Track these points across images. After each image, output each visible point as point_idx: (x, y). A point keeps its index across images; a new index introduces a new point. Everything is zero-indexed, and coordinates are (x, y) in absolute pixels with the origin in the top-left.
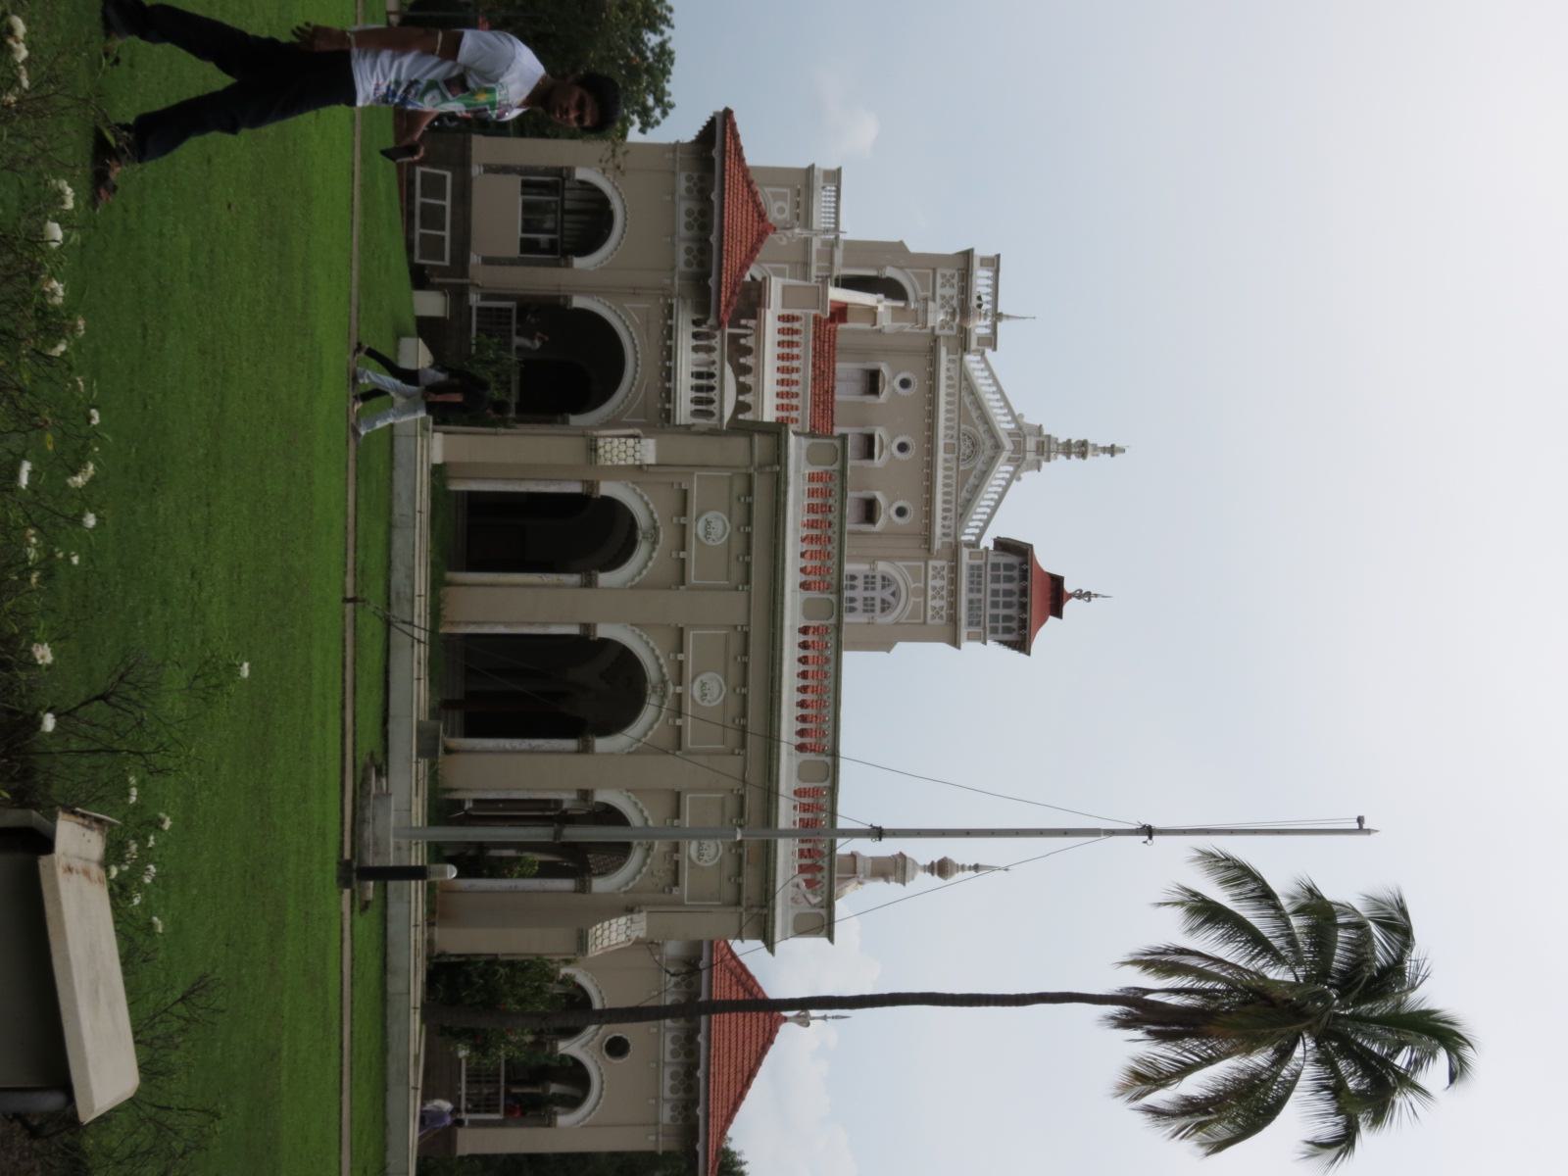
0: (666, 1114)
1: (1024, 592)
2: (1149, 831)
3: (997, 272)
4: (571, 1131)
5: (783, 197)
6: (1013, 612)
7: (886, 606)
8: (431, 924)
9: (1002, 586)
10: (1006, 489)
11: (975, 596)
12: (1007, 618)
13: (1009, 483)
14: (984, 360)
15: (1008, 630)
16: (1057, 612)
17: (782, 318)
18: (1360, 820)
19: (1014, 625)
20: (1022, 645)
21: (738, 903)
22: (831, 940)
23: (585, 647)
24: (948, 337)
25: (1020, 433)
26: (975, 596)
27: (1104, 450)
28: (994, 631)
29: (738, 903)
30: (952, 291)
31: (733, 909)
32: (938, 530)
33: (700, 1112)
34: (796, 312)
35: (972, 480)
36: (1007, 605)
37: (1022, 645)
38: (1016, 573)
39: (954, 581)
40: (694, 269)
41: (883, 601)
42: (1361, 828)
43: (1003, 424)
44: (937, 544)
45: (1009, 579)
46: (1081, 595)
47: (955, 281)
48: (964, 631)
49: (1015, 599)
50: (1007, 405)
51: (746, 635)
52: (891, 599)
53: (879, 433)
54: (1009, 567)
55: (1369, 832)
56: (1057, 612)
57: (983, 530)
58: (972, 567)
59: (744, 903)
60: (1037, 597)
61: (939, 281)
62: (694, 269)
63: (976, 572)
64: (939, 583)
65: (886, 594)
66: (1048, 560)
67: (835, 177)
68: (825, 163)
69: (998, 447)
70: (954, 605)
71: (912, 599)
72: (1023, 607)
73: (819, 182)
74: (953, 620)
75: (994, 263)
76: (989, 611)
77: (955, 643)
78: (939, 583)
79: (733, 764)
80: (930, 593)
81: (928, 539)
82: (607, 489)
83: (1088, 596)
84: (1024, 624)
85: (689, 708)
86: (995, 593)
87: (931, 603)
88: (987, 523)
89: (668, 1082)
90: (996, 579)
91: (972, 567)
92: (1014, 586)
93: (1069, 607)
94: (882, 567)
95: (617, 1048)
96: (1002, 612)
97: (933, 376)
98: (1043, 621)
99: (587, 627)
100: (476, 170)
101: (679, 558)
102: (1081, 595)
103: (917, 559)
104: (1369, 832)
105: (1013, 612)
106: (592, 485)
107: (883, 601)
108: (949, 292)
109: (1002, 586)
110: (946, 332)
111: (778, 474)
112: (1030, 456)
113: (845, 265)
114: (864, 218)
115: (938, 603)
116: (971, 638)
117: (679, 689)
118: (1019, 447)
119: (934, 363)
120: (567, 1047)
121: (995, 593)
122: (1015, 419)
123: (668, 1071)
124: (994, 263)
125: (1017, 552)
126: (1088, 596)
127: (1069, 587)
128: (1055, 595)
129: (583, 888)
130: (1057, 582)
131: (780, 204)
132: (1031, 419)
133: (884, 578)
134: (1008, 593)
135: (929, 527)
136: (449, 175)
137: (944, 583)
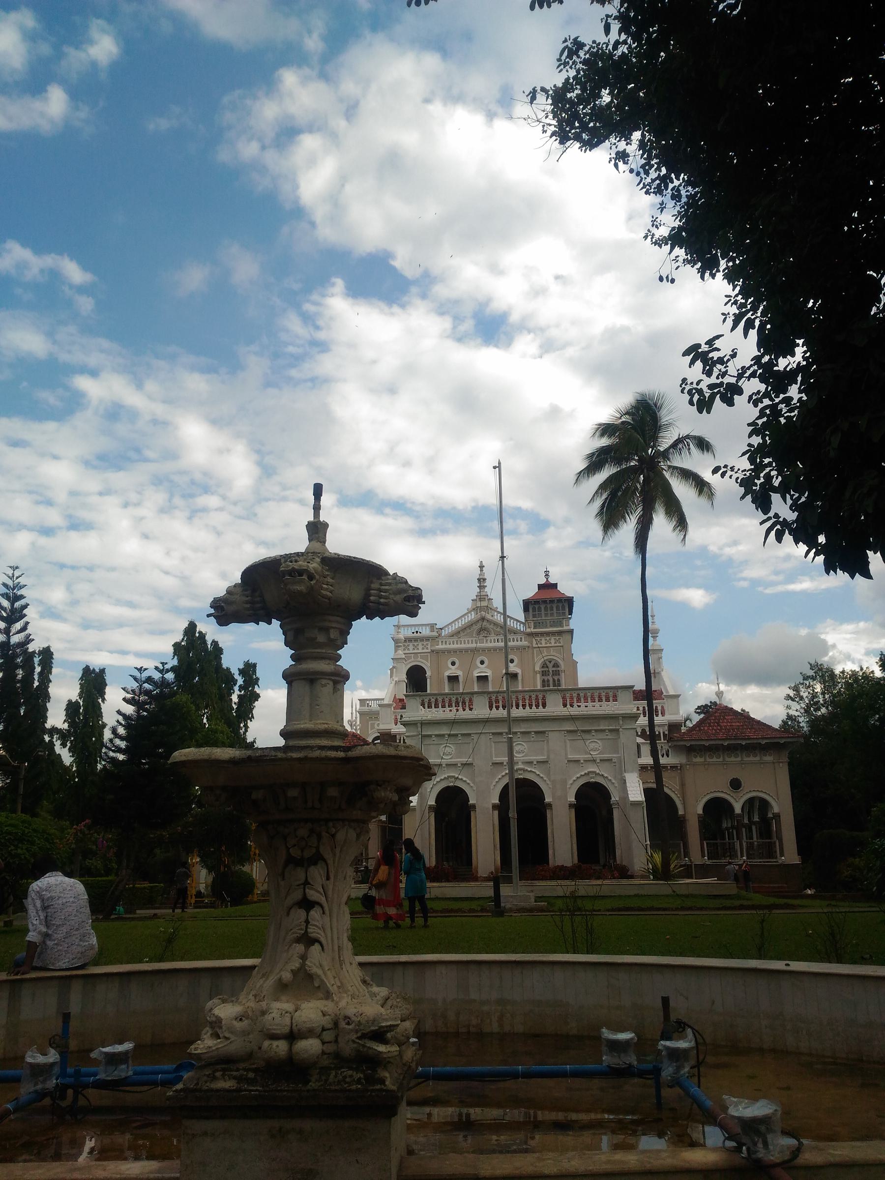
0: (768, 758)
1: (545, 602)
2: (502, 557)
4: (782, 804)
5: (372, 725)
7: (556, 665)
8: (632, 877)
9: (543, 612)
12: (558, 609)
15: (563, 609)
16: (555, 586)
18: (495, 468)
19: (560, 605)
20: (570, 601)
21: (618, 730)
23: (502, 807)
25: (475, 609)
27: (481, 570)
28: (564, 614)
29: (618, 730)
32: (519, 643)
33: (764, 742)
35: (498, 629)
36: (552, 609)
38: (537, 606)
39: (542, 634)
41: (553, 667)
42: (498, 467)
43: (473, 616)
44: (525, 643)
45: (540, 609)
46: (547, 575)
48: (565, 628)
49: (549, 606)
51: (493, 734)
52: (553, 663)
53: (476, 674)
55: (499, 463)
56: (555, 586)
58: (535, 627)
60: (548, 595)
64: (543, 642)
65: (550, 665)
66: (531, 592)
69: (483, 619)
70: (553, 634)
71: (552, 653)
72: (552, 601)
73: (366, 709)
74: (560, 633)
78: (543, 642)
79: (551, 735)
80: (548, 645)
81: (524, 648)
82: (432, 802)
85: (527, 758)
86: (546, 615)
89: (752, 758)
90: (540, 615)
91: (535, 627)
93: (552, 580)
94: (537, 668)
95: (736, 784)
97: (449, 651)
99: (495, 807)
102: (547, 575)
103: (533, 653)
104: (499, 463)
105: (554, 606)
106: (430, 807)
107: (553, 667)
109: (543, 612)
110: (429, 647)
111: (422, 724)
112: (484, 604)
115: (553, 641)
118: (481, 608)
119: (443, 651)
120: (738, 809)
121: (546, 615)
122: (469, 612)
123: (727, 759)
125: (527, 605)
127: (543, 581)
128: (548, 587)
130: (540, 587)
131: (376, 727)
132: (469, 605)
133: (543, 667)
135: (518, 648)
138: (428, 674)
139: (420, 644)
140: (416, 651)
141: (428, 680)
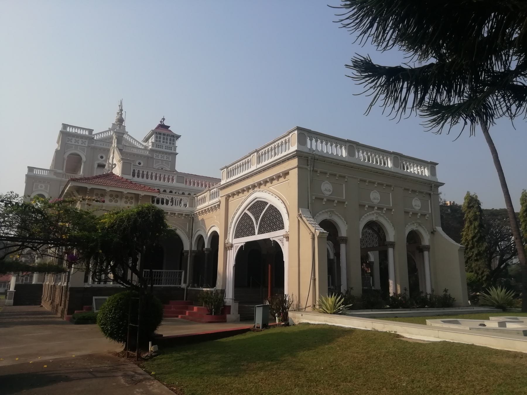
1: (164, 135)
3: (68, 125)
6: (169, 138)
9: (162, 140)
10: (130, 136)
11: (164, 147)
12: (170, 140)
13: (128, 135)
14: (96, 134)
15: (174, 140)
17: (134, 176)
19: (172, 138)
20: (178, 137)
22: (437, 164)
24: (88, 143)
26: (164, 147)
28: (173, 144)
30: (73, 140)
31: (432, 196)
34: (132, 171)
36: (167, 139)
37: (178, 137)
38: (159, 136)
39: (160, 152)
40: (133, 201)
45: (160, 138)
47: (70, 138)
48: (173, 151)
49: (165, 137)
50: (106, 132)
54: (156, 137)
57: (141, 144)
59: (430, 192)
61: (69, 142)
62: (133, 201)
63: (158, 146)
64: (160, 156)
67: (31, 169)
68: (26, 171)
70: (166, 153)
72: (168, 135)
73: (31, 174)
75: (65, 126)
76: (168, 144)
77: (177, 154)
78: (160, 156)
81: (148, 157)
83: (164, 119)
84: (173, 136)
87: (165, 159)
88: (139, 143)
92: (162, 136)
93: (166, 123)
96: (168, 141)
98: (170, 131)
100: (86, 286)
101: (337, 204)
105: (169, 138)
108: (73, 140)
109: (162, 140)
110: (87, 143)
113: (63, 170)
114: (45, 161)
115: (165, 157)
116: (175, 150)
117: (376, 208)
121: (163, 142)
122: (110, 130)
124: (65, 126)
126: (164, 119)
128: (162, 126)
129: (428, 248)
131: (39, 187)
134: (164, 139)
136: (94, 298)
137: (160, 155)
138: (84, 159)
139: (80, 140)
140: (76, 144)
141: (83, 164)
